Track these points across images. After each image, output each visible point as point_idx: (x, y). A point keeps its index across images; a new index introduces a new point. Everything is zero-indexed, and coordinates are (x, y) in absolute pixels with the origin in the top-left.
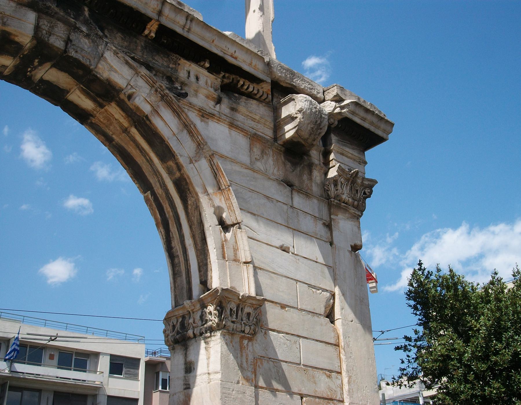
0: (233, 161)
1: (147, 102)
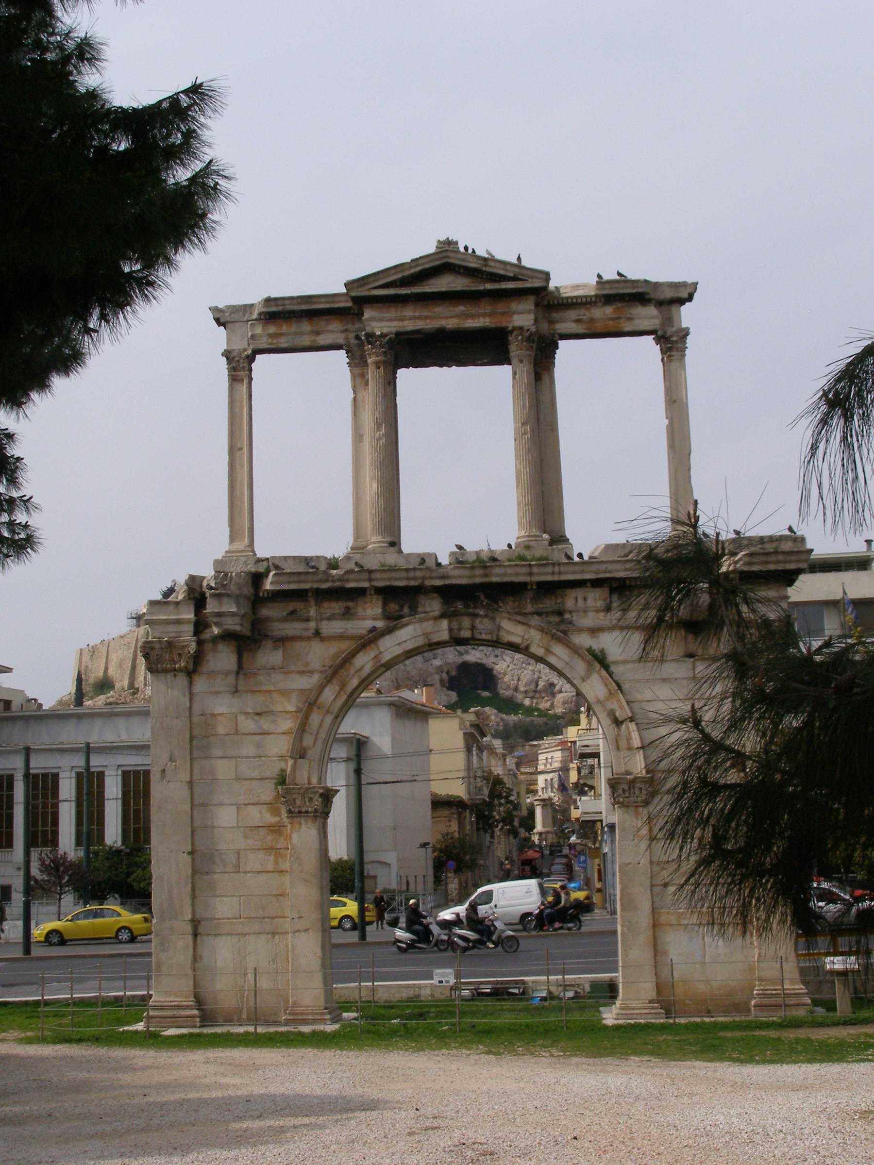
0: (624, 662)
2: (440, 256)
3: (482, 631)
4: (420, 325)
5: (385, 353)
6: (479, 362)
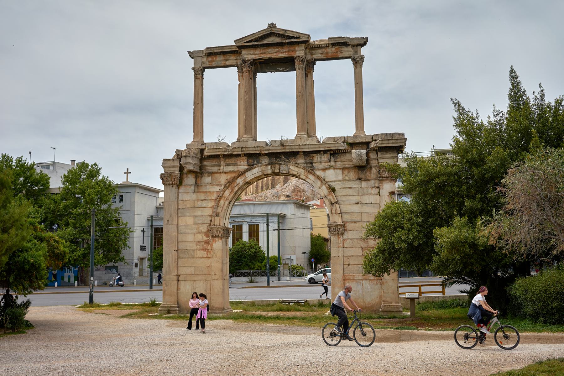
0: (335, 181)
2: (268, 30)
4: (262, 56)
5: (249, 67)
6: (285, 71)
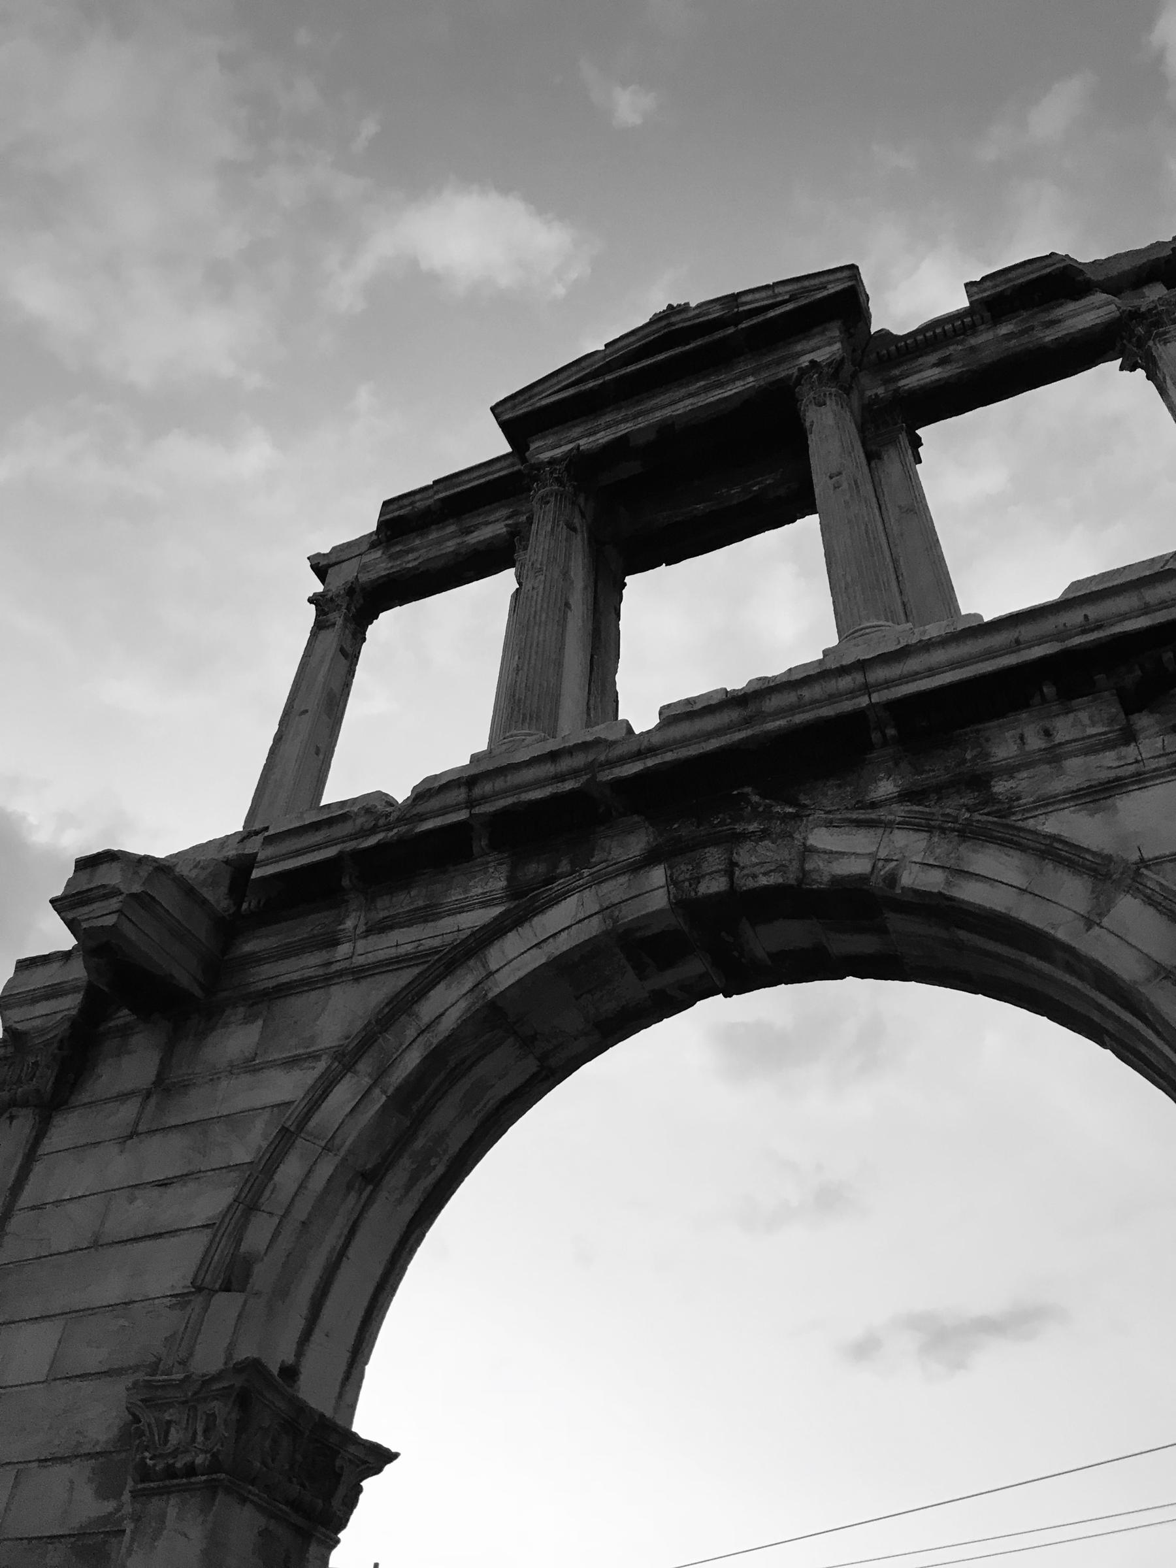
1: (927, 867)
3: (756, 870)
